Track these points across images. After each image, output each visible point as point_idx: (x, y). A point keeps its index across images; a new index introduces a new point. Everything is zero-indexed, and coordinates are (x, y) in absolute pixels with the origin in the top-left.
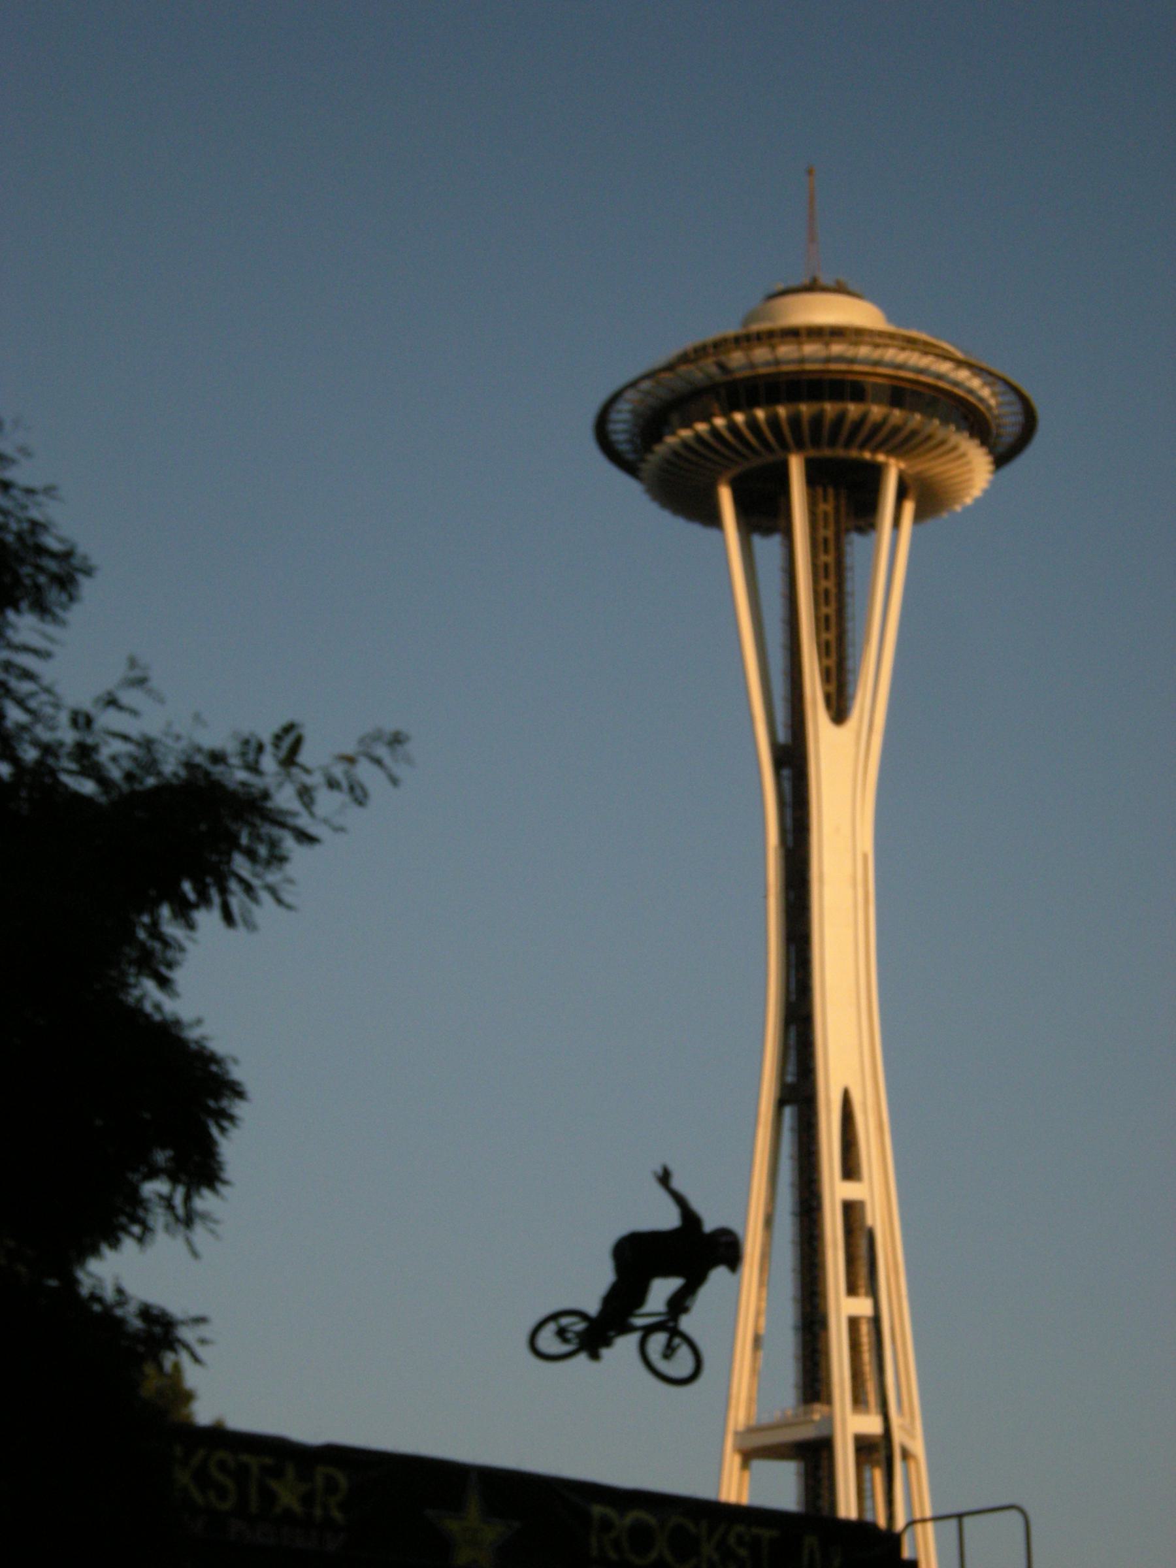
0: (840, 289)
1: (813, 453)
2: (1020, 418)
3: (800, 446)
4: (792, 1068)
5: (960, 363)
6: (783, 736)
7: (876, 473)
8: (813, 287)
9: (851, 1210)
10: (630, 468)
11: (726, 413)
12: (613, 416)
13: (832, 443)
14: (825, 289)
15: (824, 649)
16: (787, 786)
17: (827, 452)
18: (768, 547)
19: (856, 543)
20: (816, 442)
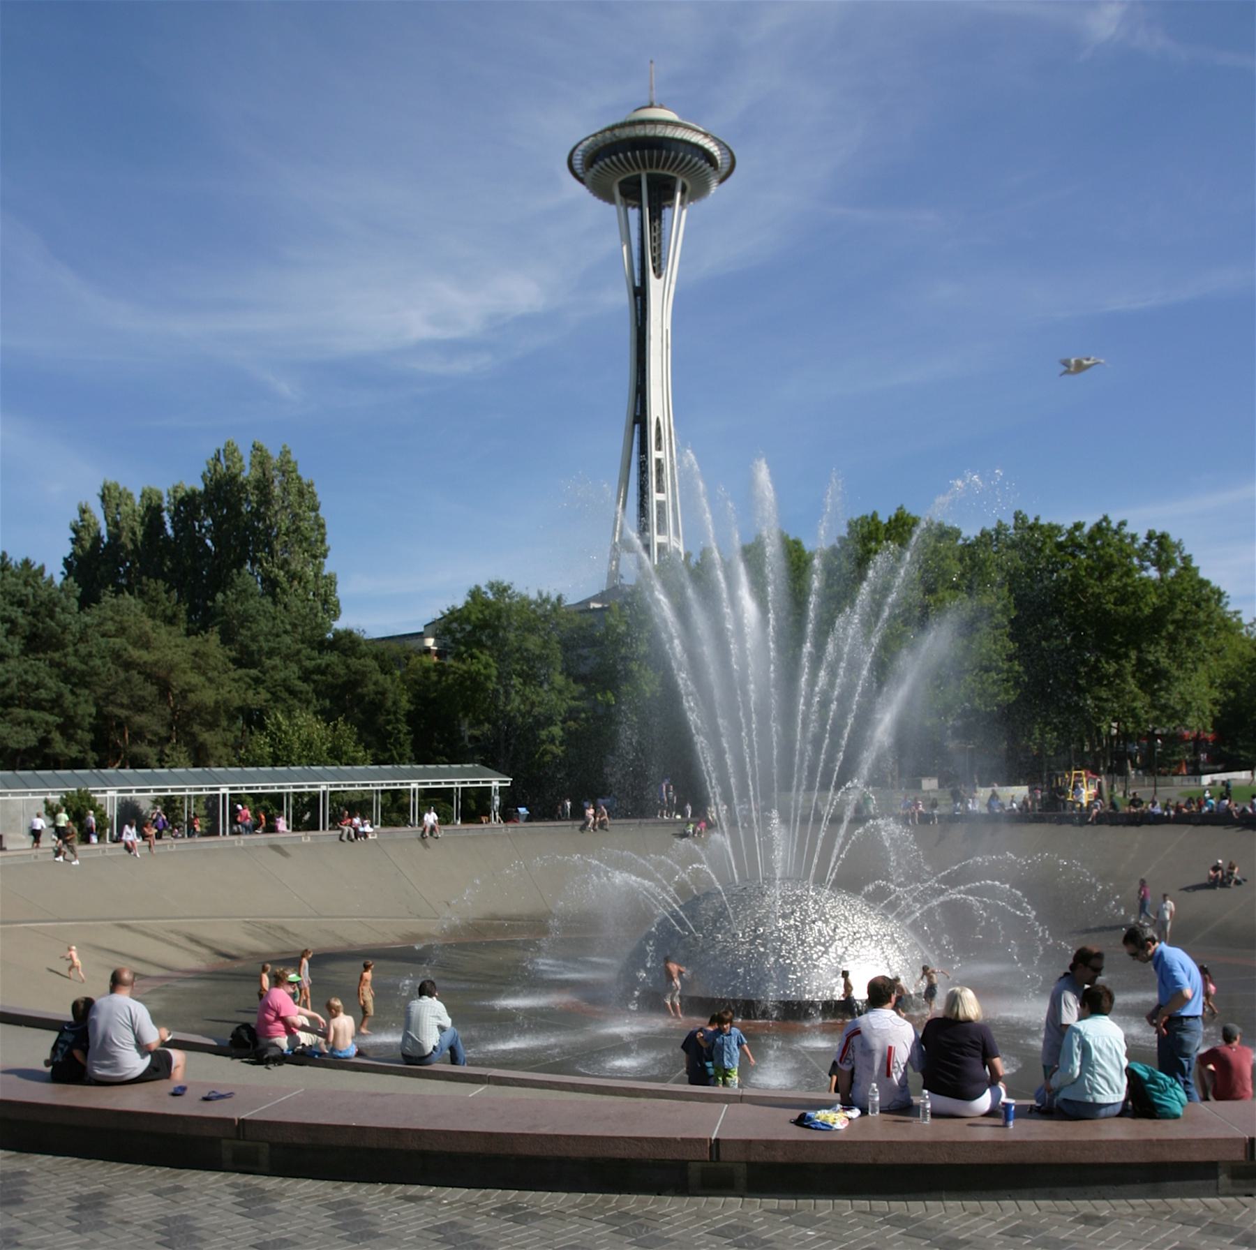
0: (661, 107)
1: (649, 171)
2: (729, 161)
3: (645, 167)
4: (639, 410)
5: (706, 135)
6: (637, 284)
7: (674, 179)
8: (651, 106)
9: (658, 461)
10: (581, 180)
11: (616, 154)
12: (575, 157)
13: (657, 167)
14: (656, 107)
15: (654, 250)
16: (639, 303)
17: (654, 171)
18: (634, 214)
19: (666, 213)
20: (651, 166)
